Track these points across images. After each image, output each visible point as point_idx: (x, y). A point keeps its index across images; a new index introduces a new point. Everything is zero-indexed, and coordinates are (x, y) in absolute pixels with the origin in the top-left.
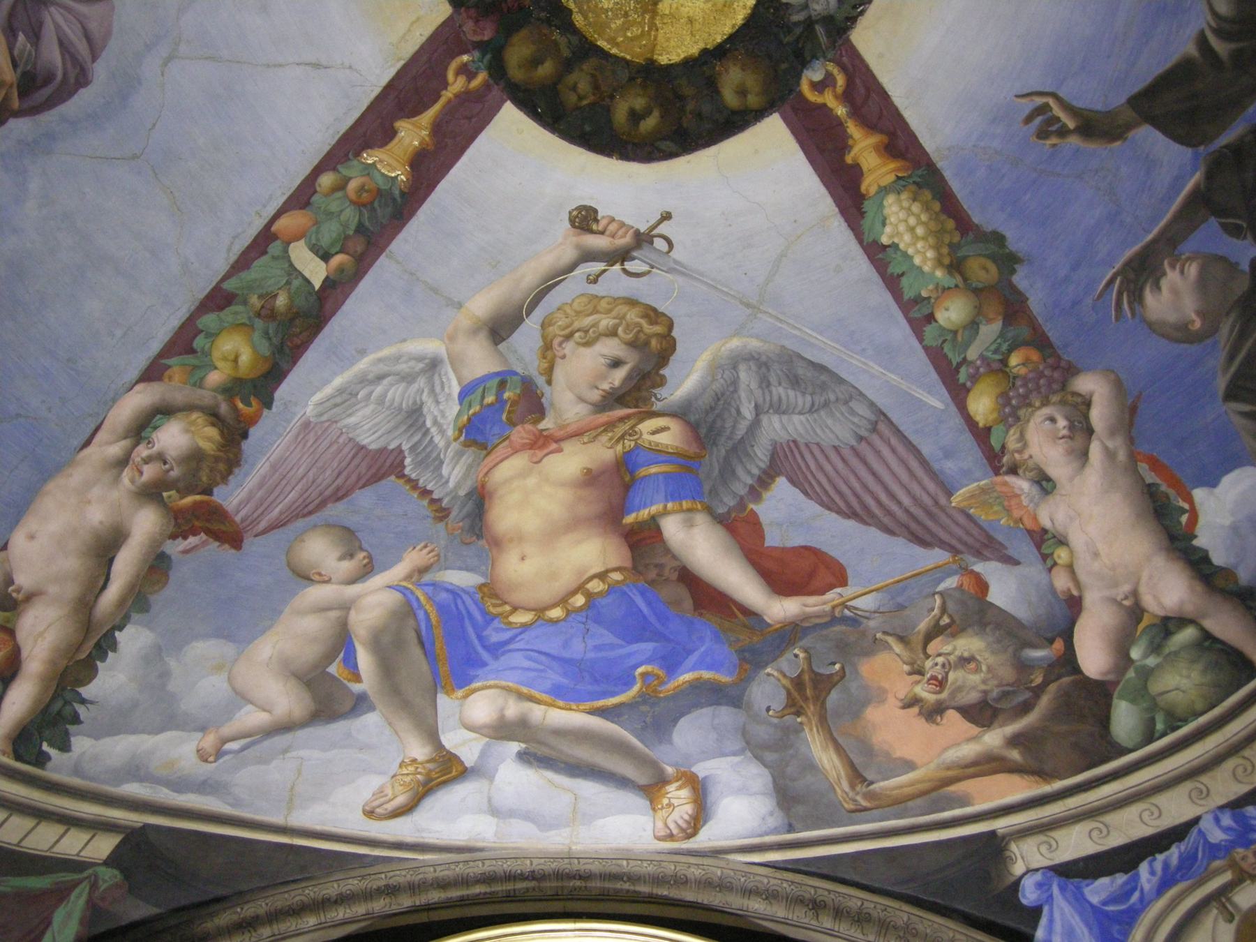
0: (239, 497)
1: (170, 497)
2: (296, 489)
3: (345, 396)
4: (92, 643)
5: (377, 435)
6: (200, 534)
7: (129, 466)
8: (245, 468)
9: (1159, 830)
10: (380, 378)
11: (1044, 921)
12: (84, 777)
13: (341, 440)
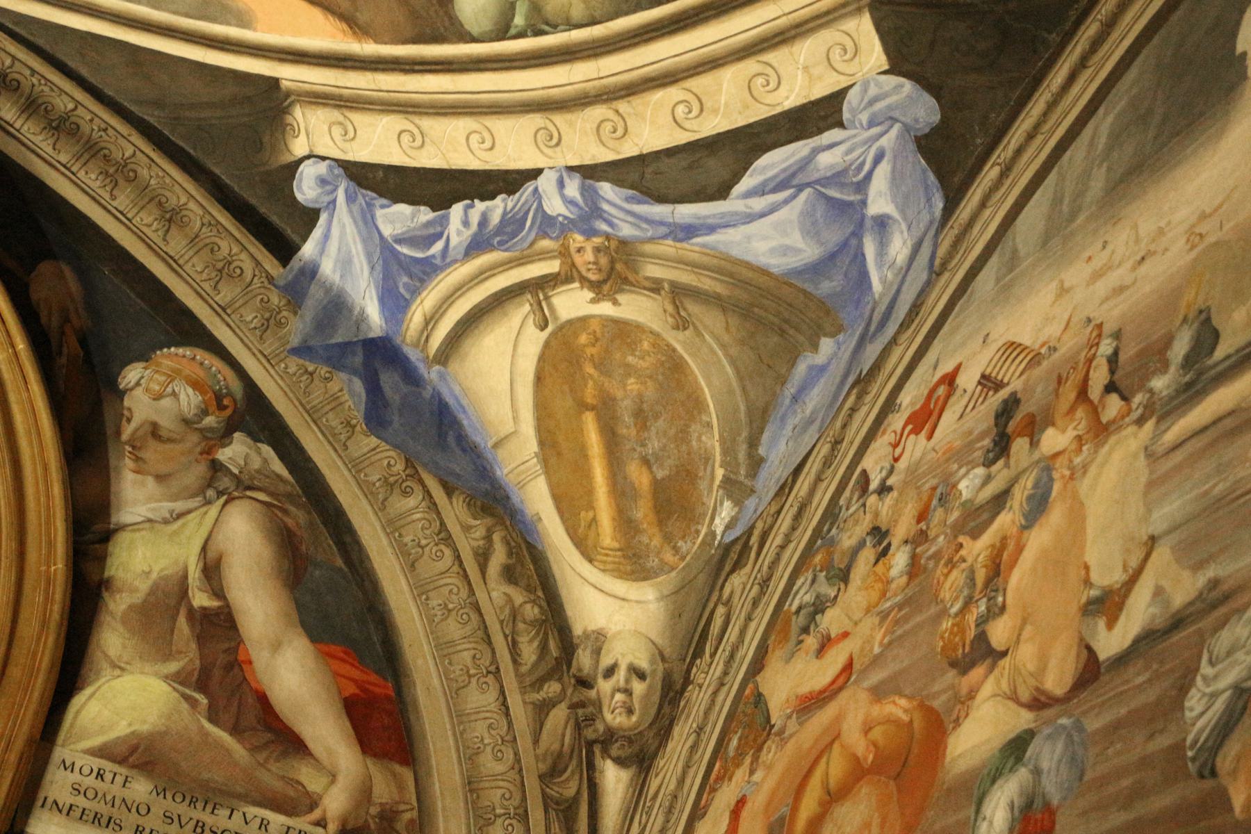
9: (487, 167)
11: (317, 233)
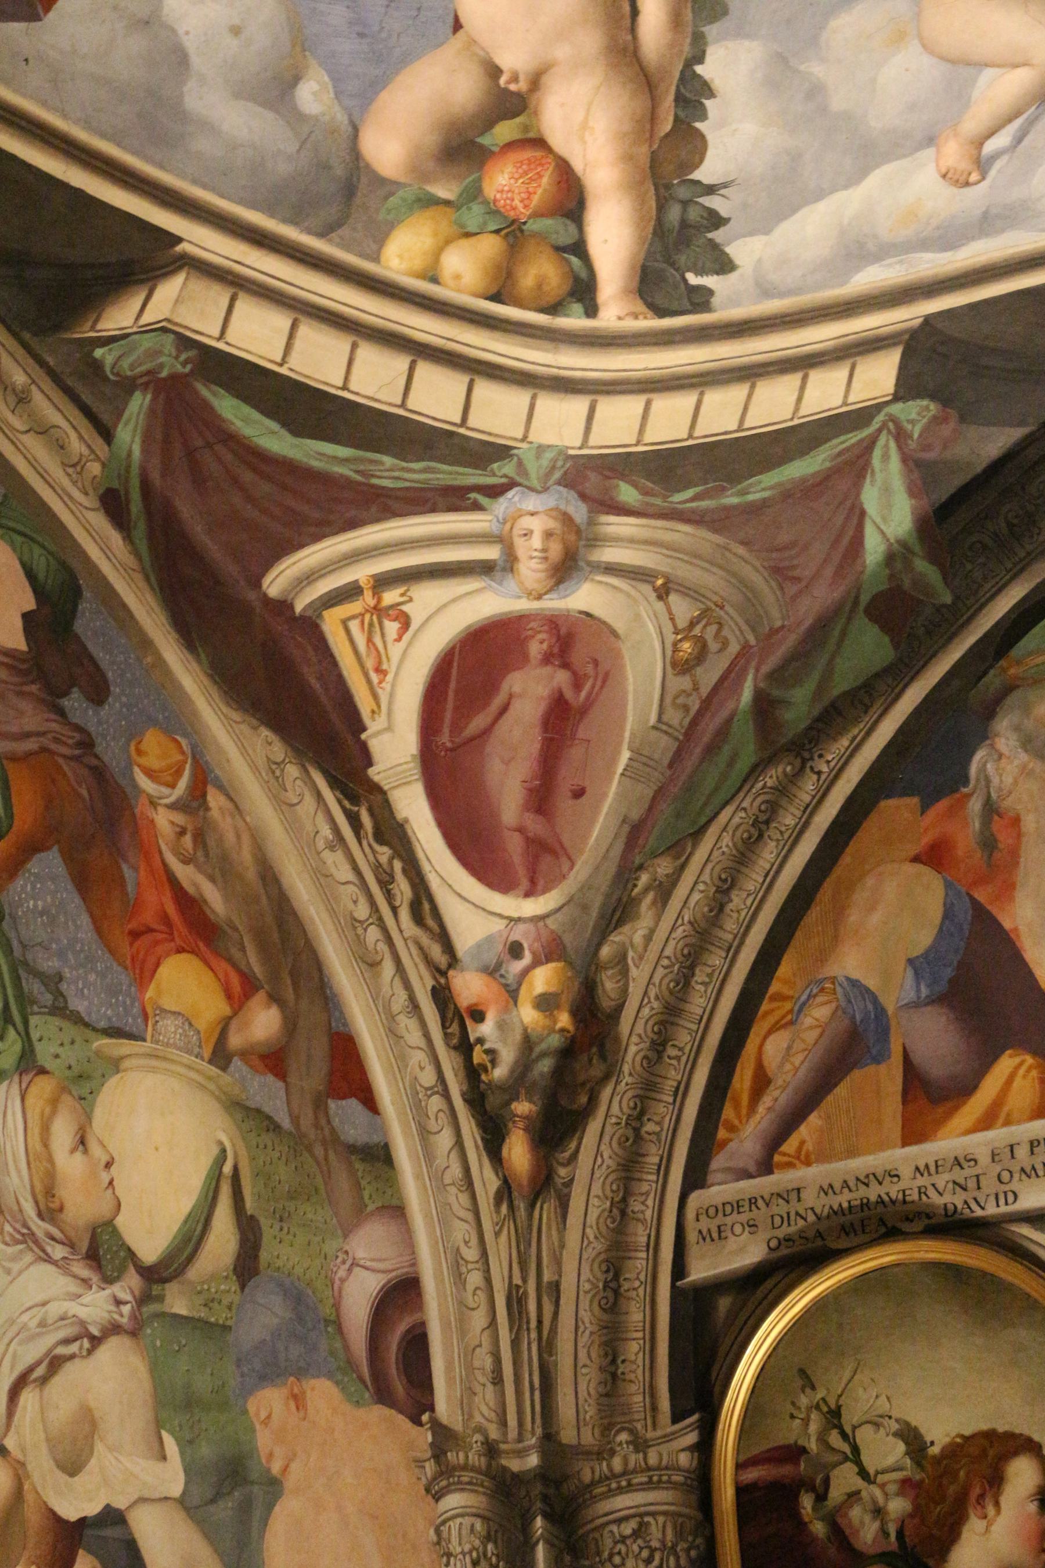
12: (782, 295)
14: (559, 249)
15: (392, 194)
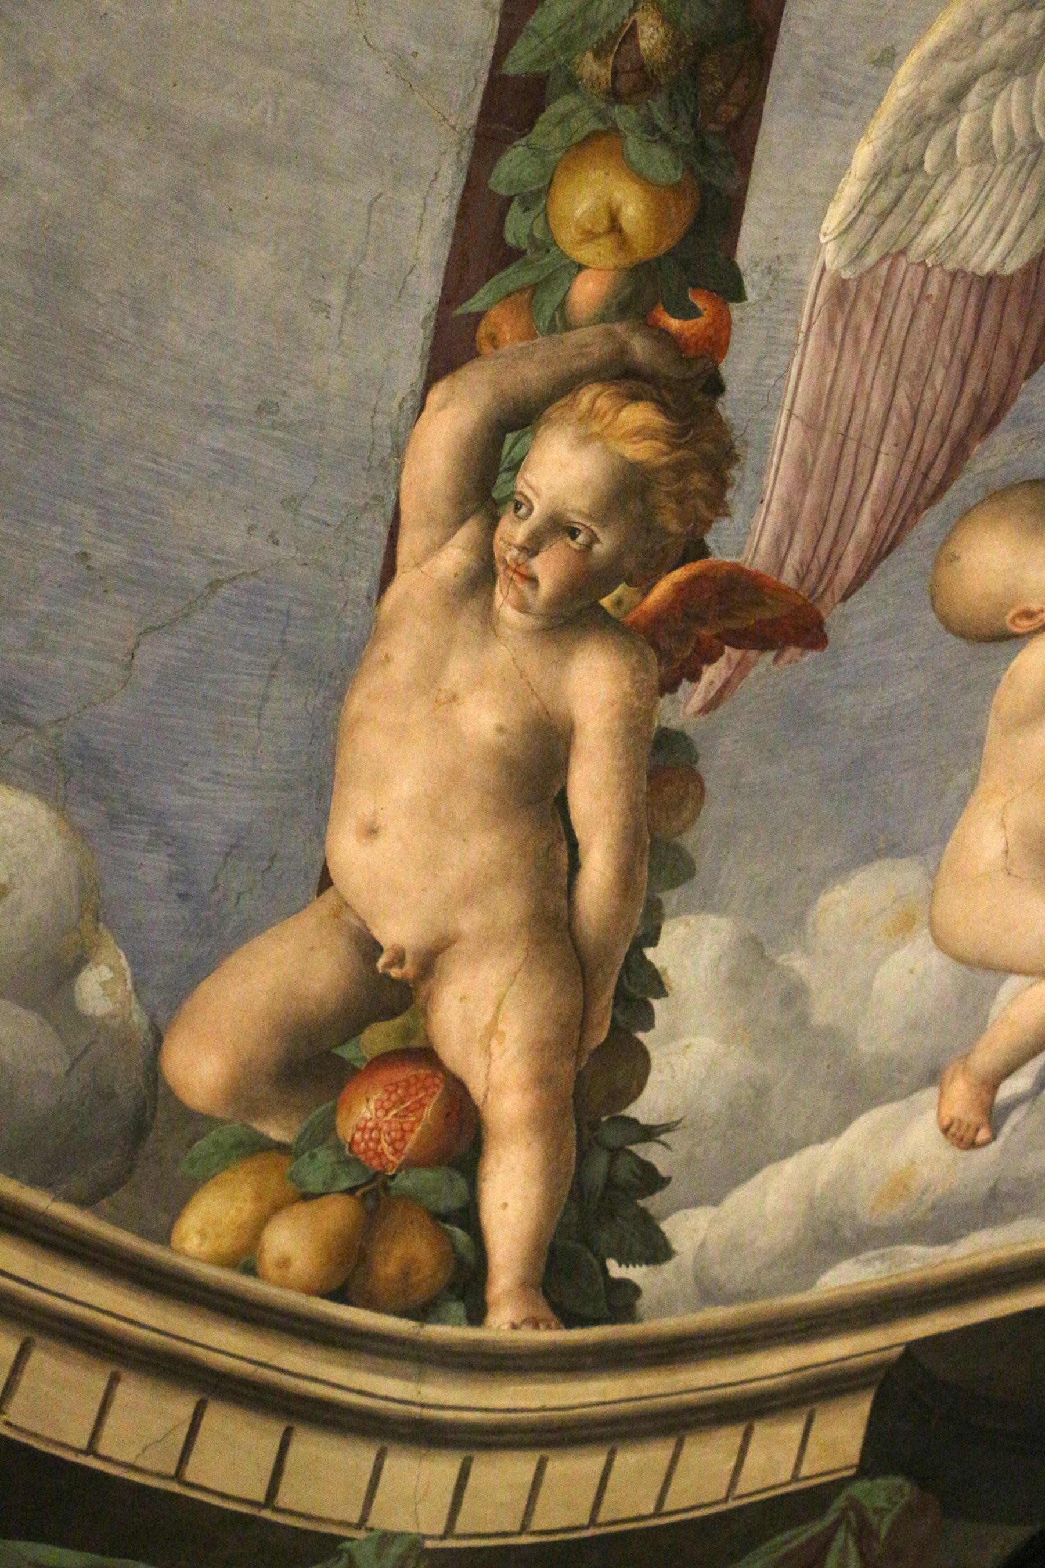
0: (769, 527)
1: (619, 603)
2: (884, 449)
3: (895, 182)
4: (606, 998)
5: (1008, 237)
6: (721, 653)
7: (501, 578)
8: (750, 457)
10: (955, 97)
12: (729, 1300)
13: (933, 289)
14: (440, 1217)
15: (197, 1136)
